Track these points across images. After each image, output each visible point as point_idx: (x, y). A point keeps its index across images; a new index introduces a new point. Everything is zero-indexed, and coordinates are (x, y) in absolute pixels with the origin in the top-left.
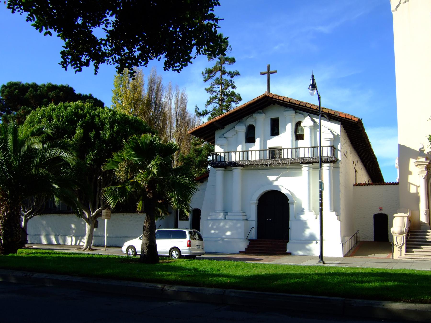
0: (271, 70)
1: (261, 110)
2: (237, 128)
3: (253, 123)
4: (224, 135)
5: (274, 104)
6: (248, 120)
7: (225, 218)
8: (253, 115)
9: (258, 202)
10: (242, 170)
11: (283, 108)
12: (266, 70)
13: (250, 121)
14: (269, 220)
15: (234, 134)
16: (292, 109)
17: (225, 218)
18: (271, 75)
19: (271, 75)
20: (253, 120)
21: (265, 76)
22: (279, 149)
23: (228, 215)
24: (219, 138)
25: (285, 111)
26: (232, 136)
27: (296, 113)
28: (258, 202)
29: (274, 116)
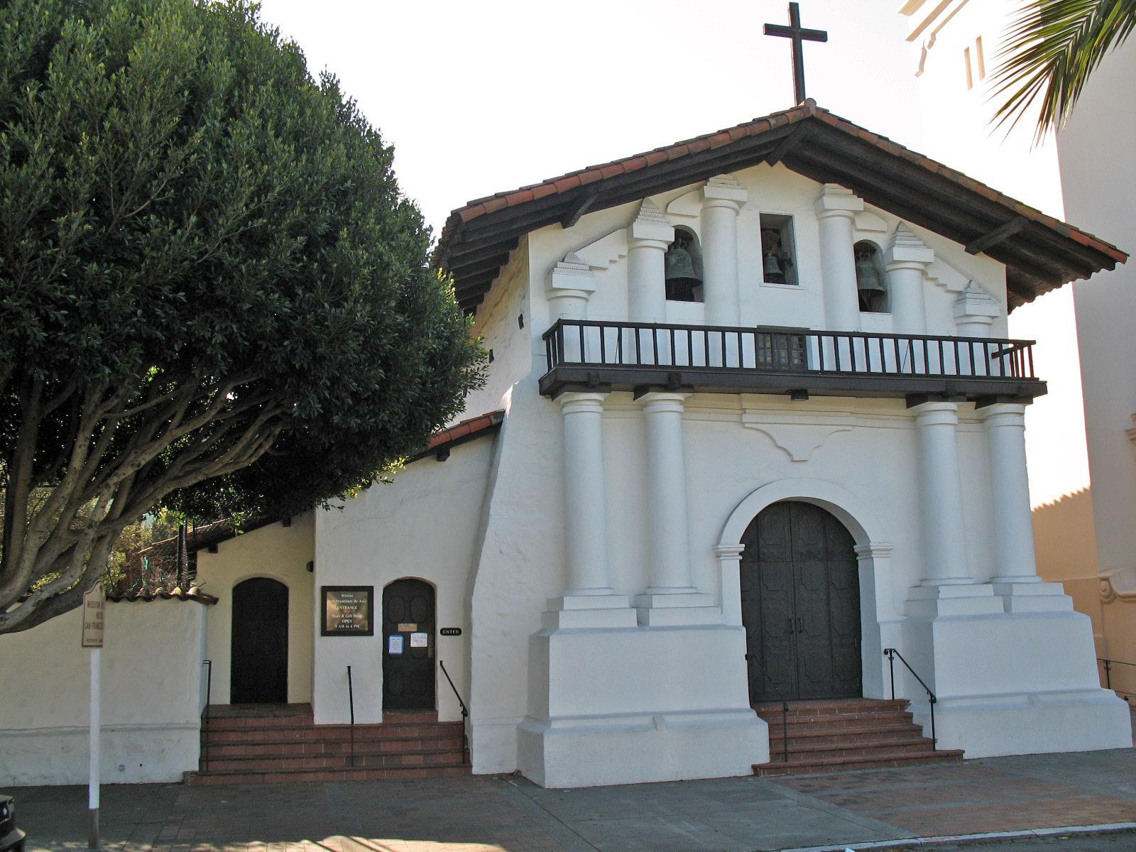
0: (805, 24)
3: (695, 225)
4: (581, 254)
5: (772, 164)
9: (744, 545)
11: (804, 184)
12: (785, 21)
15: (621, 256)
18: (788, 42)
19: (788, 42)
20: (696, 209)
22: (801, 335)
24: (559, 264)
26: (611, 262)
28: (744, 545)
29: (777, 207)
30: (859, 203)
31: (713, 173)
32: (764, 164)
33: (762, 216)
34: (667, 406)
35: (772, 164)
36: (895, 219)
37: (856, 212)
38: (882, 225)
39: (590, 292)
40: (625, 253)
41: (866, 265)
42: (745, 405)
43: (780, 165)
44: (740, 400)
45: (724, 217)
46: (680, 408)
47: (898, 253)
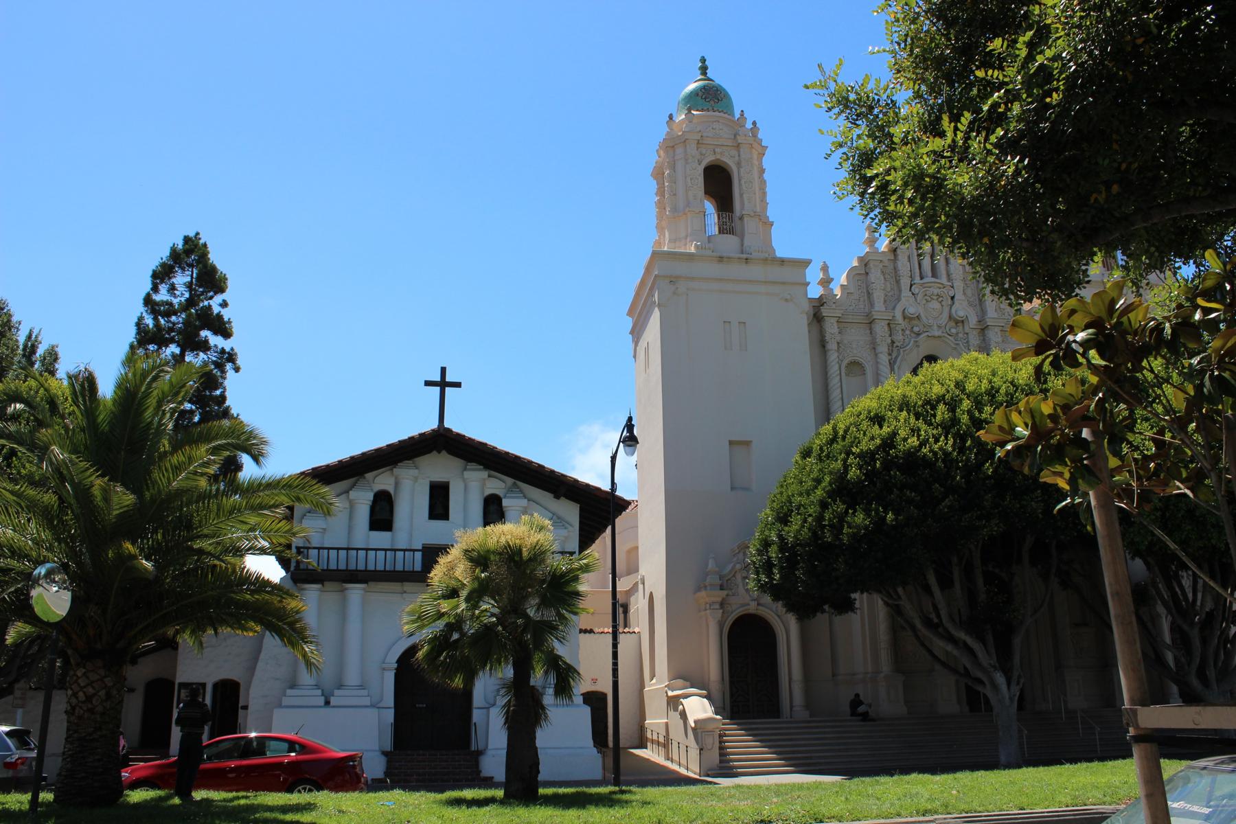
1: (411, 462)
2: (353, 494)
3: (391, 489)
5: (439, 452)
6: (378, 480)
7: (327, 703)
8: (395, 469)
10: (366, 591)
11: (457, 463)
12: (438, 378)
13: (383, 481)
14: (421, 706)
16: (482, 467)
17: (327, 703)
21: (438, 389)
23: (333, 696)
24: (308, 514)
25: (465, 469)
27: (489, 476)
29: (439, 477)
30: (485, 474)
31: (401, 461)
32: (435, 452)
33: (431, 482)
34: (356, 592)
35: (439, 452)
36: (510, 481)
37: (484, 479)
38: (503, 485)
39: (324, 529)
40: (347, 505)
41: (493, 508)
42: (405, 589)
43: (444, 452)
44: (402, 585)
45: (406, 484)
46: (362, 592)
47: (505, 502)
